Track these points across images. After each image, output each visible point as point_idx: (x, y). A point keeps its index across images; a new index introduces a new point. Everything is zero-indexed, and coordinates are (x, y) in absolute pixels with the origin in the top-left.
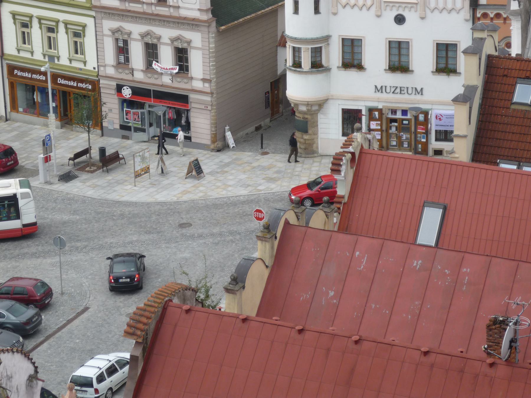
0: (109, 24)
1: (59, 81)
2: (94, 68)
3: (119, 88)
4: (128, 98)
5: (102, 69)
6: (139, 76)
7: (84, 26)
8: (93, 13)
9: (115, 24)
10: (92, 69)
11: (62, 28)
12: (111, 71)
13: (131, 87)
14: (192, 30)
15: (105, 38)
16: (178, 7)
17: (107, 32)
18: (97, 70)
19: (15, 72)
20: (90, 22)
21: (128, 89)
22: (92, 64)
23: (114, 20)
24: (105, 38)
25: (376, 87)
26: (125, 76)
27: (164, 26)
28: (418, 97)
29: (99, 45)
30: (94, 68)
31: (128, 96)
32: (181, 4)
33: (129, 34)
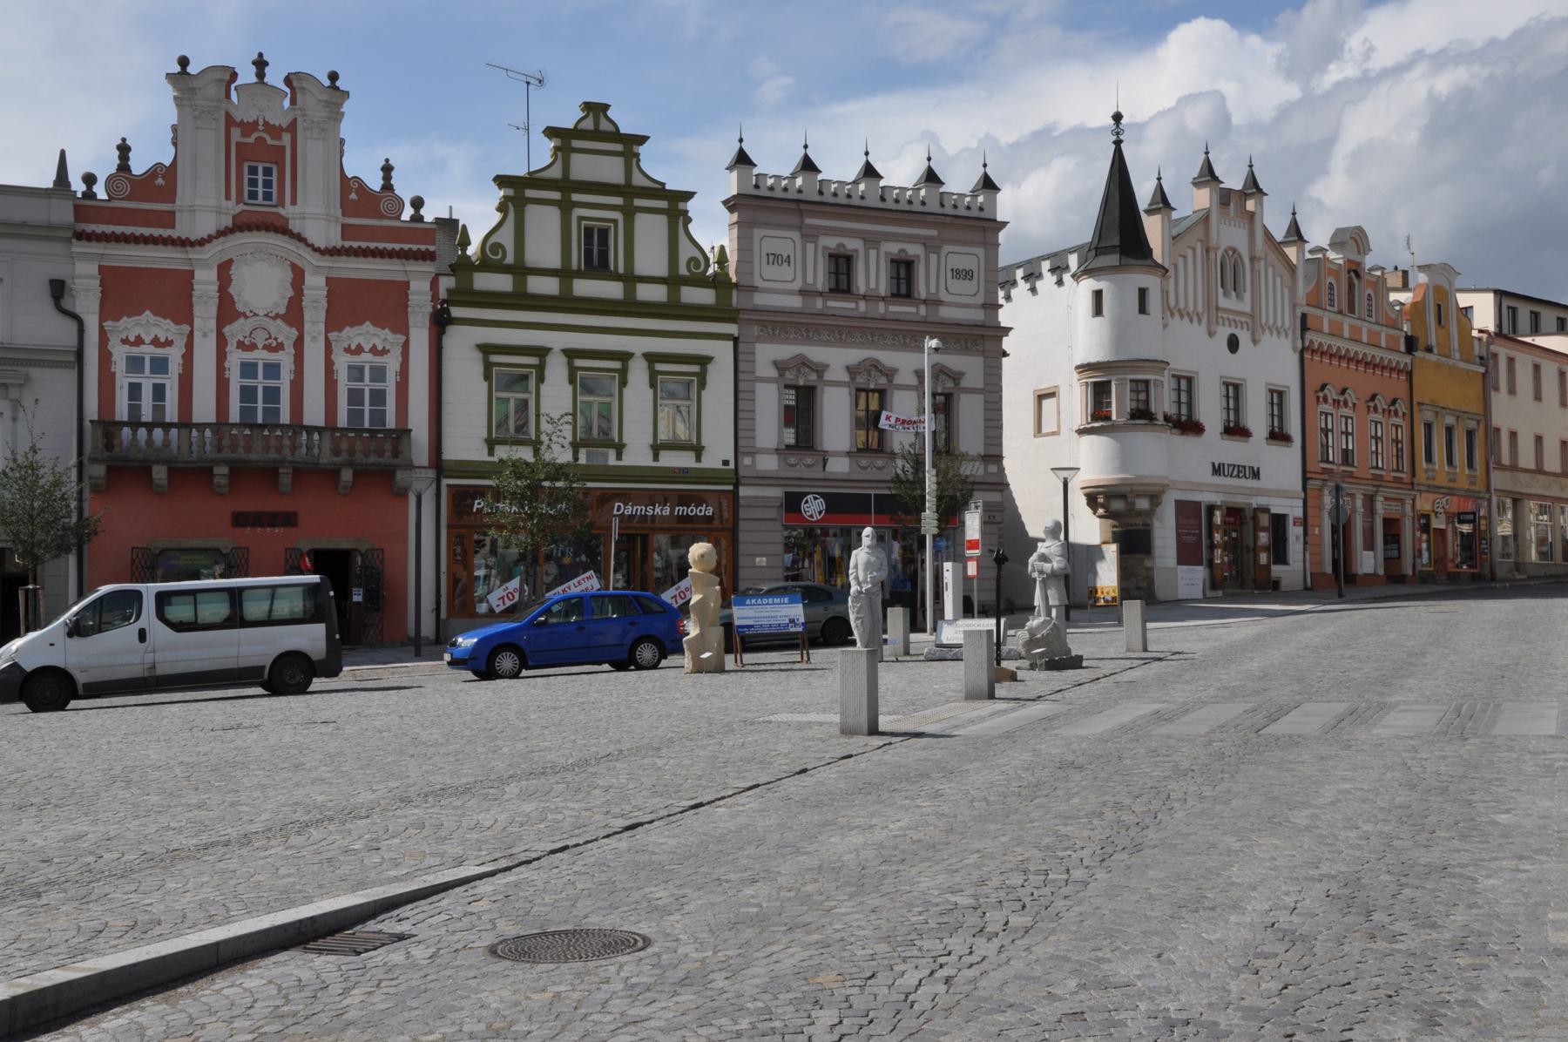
1: (618, 510)
3: (793, 503)
4: (818, 521)
5: (747, 461)
6: (839, 466)
7: (704, 361)
8: (732, 329)
9: (786, 351)
10: (719, 465)
12: (768, 464)
13: (823, 495)
14: (965, 350)
15: (759, 387)
16: (939, 303)
18: (732, 466)
19: (476, 506)
20: (722, 353)
22: (718, 452)
24: (759, 387)
25: (1213, 464)
28: (1252, 483)
29: (741, 405)
30: (726, 463)
31: (817, 517)
32: (943, 296)
33: (820, 369)
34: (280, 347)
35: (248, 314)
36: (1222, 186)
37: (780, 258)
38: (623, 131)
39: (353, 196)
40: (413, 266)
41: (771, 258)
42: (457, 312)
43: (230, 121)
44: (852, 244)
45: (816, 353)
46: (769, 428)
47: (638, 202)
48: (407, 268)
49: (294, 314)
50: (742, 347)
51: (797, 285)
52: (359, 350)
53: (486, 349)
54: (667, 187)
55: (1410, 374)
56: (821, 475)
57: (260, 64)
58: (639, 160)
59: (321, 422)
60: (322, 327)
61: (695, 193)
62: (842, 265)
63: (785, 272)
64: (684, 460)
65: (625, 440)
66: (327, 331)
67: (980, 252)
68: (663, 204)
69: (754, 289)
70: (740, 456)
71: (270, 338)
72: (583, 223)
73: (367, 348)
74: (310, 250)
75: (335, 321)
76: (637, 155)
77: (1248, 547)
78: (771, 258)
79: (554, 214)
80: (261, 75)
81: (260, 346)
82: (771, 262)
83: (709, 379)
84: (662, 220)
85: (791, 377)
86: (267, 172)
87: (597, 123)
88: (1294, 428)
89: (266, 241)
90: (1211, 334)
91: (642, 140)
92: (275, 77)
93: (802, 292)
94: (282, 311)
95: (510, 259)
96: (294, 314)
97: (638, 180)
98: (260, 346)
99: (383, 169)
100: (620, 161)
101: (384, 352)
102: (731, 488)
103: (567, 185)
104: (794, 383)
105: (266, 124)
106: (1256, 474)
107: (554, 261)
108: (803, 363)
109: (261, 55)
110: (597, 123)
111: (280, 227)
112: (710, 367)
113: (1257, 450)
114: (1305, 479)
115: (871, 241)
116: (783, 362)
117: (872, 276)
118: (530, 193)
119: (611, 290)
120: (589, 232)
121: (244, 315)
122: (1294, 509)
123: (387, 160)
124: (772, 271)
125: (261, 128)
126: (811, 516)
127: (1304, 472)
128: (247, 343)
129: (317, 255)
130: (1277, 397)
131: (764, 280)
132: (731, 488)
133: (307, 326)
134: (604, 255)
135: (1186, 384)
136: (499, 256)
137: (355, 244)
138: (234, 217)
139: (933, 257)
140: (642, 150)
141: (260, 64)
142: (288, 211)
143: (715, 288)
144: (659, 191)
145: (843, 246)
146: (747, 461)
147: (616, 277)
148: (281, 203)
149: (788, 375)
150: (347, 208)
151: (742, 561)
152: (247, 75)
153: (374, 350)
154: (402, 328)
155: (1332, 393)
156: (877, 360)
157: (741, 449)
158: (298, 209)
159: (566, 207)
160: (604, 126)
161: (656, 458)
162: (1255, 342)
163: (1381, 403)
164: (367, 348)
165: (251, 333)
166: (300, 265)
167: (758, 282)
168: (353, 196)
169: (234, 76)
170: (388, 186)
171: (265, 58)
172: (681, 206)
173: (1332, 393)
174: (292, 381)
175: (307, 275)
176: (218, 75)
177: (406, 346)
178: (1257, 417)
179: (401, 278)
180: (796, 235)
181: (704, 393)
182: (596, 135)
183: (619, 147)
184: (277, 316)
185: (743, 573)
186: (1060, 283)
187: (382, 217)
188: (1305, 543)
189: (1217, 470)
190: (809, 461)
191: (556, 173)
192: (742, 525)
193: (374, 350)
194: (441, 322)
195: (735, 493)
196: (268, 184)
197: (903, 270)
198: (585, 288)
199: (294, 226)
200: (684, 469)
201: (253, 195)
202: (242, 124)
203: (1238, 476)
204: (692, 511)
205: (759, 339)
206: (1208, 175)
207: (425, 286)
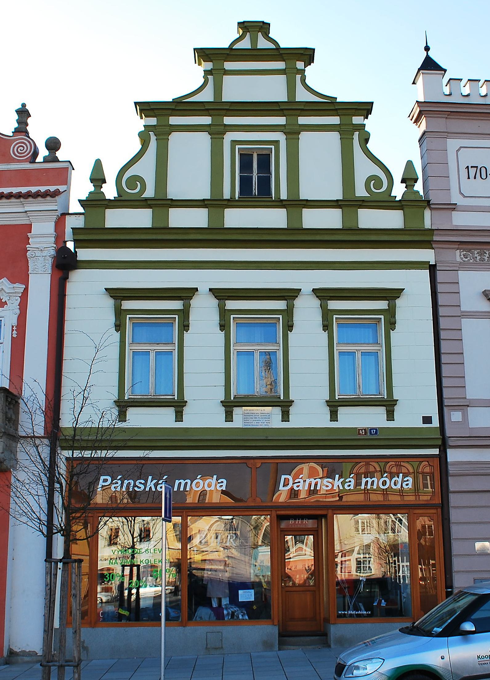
5: (455, 416)
10: (420, 424)
15: (466, 323)
18: (436, 423)
24: (466, 323)
29: (445, 347)
30: (427, 420)
37: (483, 170)
38: (282, 46)
40: (32, 206)
41: (472, 171)
47: (303, 120)
48: (27, 209)
50: (441, 277)
54: (338, 100)
68: (335, 120)
69: (453, 207)
70: (446, 409)
72: (237, 147)
78: (472, 171)
82: (472, 175)
83: (399, 316)
87: (254, 41)
95: (149, 193)
97: (302, 96)
99: (18, 112)
100: (282, 78)
102: (436, 451)
110: (254, 41)
112: (398, 302)
118: (174, 120)
131: (465, 197)
132: (436, 451)
134: (265, 183)
147: (280, 204)
151: (456, 548)
157: (446, 402)
160: (263, 44)
161: (334, 416)
167: (456, 199)
172: (357, 120)
179: (22, 220)
185: (457, 564)
187: (13, 161)
191: (207, 96)
192: (453, 499)
195: (442, 458)
200: (371, 429)
204: (384, 483)
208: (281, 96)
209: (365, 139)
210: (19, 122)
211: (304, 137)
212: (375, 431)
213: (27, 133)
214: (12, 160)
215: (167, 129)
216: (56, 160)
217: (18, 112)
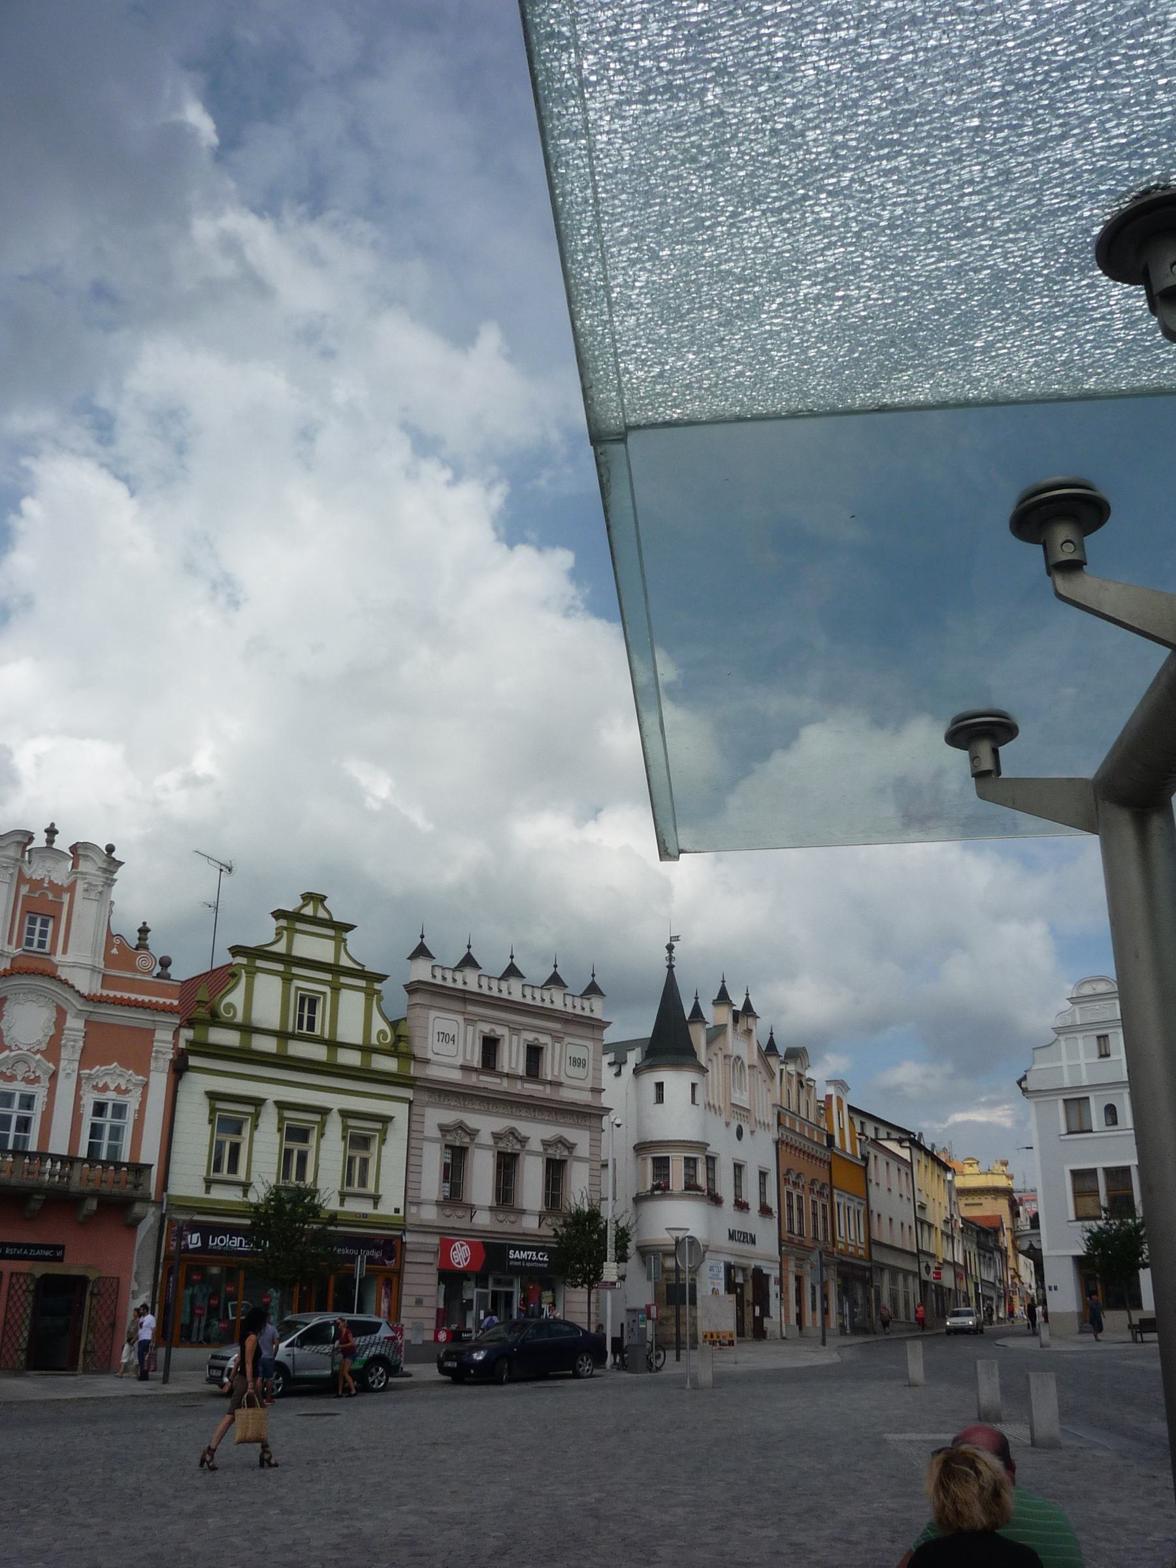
0: (437, 1116)
2: (397, 1211)
6: (483, 1220)
8: (408, 1093)
9: (449, 1116)
10: (392, 1213)
11: (334, 1127)
12: (429, 1214)
13: (468, 1243)
16: (560, 1084)
17: (432, 1131)
18: (402, 1213)
20: (399, 1112)
21: (464, 1248)
22: (392, 1201)
23: (449, 1107)
26: (457, 1221)
27: (533, 1120)
30: (397, 1211)
32: (563, 1079)
34: (37, 1080)
35: (13, 1048)
36: (734, 1008)
39: (115, 951)
42: (193, 1061)
43: (22, 879)
44: (500, 1031)
45: (473, 1120)
46: (432, 1185)
47: (344, 980)
49: (52, 1050)
50: (415, 1110)
51: (459, 1061)
52: (105, 1088)
53: (213, 1096)
55: (830, 1164)
56: (467, 1225)
57: (51, 832)
58: (345, 945)
59: (64, 1151)
60: (77, 1064)
61: (388, 976)
62: (490, 1045)
63: (449, 1049)
64: (364, 1207)
65: (319, 1187)
66: (81, 1067)
67: (590, 1044)
69: (426, 1061)
70: (408, 1204)
71: (29, 1071)
73: (112, 1087)
74: (76, 995)
75: (87, 1059)
76: (345, 940)
77: (748, 1301)
79: (277, 982)
80: (50, 841)
81: (20, 1078)
84: (361, 996)
85: (451, 1138)
86: (45, 924)
87: (316, 910)
88: (772, 1202)
89: (52, 988)
90: (727, 1124)
91: (349, 928)
92: (62, 843)
93: (464, 1068)
94: (43, 1047)
95: (239, 1018)
96: (52, 1050)
97: (345, 962)
98: (20, 1078)
100: (331, 944)
101: (127, 1091)
103: (289, 960)
104: (453, 1143)
105: (51, 882)
106: (753, 1242)
107: (275, 1023)
108: (461, 1127)
109: (53, 825)
111: (51, 975)
112: (390, 1126)
113: (753, 1222)
114: (780, 1246)
115: (515, 1030)
116: (447, 1126)
117: (512, 1058)
118: (260, 963)
119: (319, 1053)
120: (302, 999)
121: (9, 1048)
122: (775, 1273)
123: (144, 923)
124: (440, 1047)
125: (46, 885)
126: (459, 1263)
127: (780, 1240)
128: (8, 1074)
129: (82, 1000)
130: (763, 1175)
133: (63, 1064)
135: (711, 1160)
136: (231, 1015)
137: (112, 994)
138: (13, 960)
139: (557, 1045)
140: (348, 936)
141: (51, 832)
142: (58, 958)
143: (397, 1057)
144: (359, 973)
145: (493, 1030)
146: (413, 1209)
147: (318, 1040)
148: (53, 951)
149: (448, 1137)
150: (109, 960)
152: (40, 841)
153: (118, 1089)
154: (143, 1069)
155: (792, 1178)
156: (514, 1129)
158: (70, 958)
159: (287, 979)
160: (322, 914)
162: (752, 1132)
163: (817, 1188)
164: (112, 1087)
165: (13, 1066)
166: (65, 1007)
167: (430, 1056)
168: (115, 951)
169: (31, 839)
170: (142, 945)
171: (56, 827)
172: (377, 986)
173: (792, 1178)
174: (43, 1112)
175: (68, 1017)
176: (19, 838)
177: (146, 1086)
178: (751, 1195)
179: (150, 1026)
180: (460, 1018)
181: (383, 1148)
182: (314, 920)
183: (331, 932)
184: (38, 1051)
186: (618, 1074)
188: (781, 1299)
189: (732, 1236)
190: (460, 1213)
191: (281, 948)
193: (118, 1089)
194: (179, 1068)
196: (43, 934)
197: (534, 1053)
198: (297, 1049)
199: (63, 973)
201: (30, 942)
202: (30, 881)
203: (743, 1241)
205: (427, 1105)
206: (723, 998)
207: (169, 1036)
208: (329, 958)
209: (380, 999)
210: (140, 939)
211: (345, 994)
212: (365, 1215)
213: (146, 948)
214: (134, 970)
215: (254, 970)
216: (168, 977)
217: (140, 931)
